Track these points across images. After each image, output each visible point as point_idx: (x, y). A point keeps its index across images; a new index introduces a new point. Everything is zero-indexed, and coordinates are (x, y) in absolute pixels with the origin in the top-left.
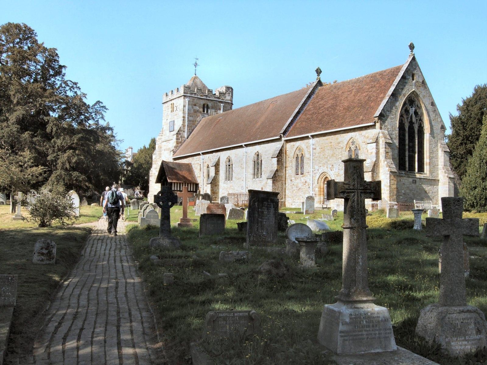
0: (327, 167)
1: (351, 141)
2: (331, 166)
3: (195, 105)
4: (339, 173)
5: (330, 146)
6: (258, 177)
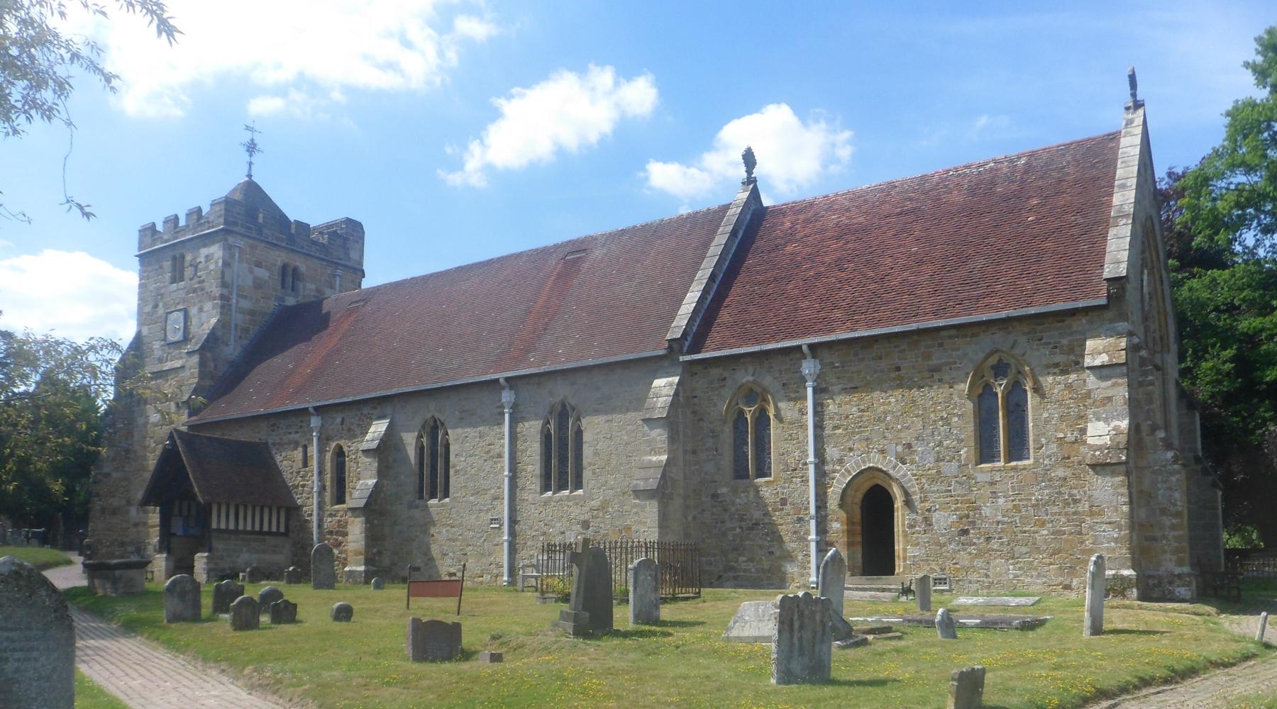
0: (882, 451)
1: (993, 360)
2: (900, 448)
3: (259, 265)
4: (939, 472)
6: (562, 486)
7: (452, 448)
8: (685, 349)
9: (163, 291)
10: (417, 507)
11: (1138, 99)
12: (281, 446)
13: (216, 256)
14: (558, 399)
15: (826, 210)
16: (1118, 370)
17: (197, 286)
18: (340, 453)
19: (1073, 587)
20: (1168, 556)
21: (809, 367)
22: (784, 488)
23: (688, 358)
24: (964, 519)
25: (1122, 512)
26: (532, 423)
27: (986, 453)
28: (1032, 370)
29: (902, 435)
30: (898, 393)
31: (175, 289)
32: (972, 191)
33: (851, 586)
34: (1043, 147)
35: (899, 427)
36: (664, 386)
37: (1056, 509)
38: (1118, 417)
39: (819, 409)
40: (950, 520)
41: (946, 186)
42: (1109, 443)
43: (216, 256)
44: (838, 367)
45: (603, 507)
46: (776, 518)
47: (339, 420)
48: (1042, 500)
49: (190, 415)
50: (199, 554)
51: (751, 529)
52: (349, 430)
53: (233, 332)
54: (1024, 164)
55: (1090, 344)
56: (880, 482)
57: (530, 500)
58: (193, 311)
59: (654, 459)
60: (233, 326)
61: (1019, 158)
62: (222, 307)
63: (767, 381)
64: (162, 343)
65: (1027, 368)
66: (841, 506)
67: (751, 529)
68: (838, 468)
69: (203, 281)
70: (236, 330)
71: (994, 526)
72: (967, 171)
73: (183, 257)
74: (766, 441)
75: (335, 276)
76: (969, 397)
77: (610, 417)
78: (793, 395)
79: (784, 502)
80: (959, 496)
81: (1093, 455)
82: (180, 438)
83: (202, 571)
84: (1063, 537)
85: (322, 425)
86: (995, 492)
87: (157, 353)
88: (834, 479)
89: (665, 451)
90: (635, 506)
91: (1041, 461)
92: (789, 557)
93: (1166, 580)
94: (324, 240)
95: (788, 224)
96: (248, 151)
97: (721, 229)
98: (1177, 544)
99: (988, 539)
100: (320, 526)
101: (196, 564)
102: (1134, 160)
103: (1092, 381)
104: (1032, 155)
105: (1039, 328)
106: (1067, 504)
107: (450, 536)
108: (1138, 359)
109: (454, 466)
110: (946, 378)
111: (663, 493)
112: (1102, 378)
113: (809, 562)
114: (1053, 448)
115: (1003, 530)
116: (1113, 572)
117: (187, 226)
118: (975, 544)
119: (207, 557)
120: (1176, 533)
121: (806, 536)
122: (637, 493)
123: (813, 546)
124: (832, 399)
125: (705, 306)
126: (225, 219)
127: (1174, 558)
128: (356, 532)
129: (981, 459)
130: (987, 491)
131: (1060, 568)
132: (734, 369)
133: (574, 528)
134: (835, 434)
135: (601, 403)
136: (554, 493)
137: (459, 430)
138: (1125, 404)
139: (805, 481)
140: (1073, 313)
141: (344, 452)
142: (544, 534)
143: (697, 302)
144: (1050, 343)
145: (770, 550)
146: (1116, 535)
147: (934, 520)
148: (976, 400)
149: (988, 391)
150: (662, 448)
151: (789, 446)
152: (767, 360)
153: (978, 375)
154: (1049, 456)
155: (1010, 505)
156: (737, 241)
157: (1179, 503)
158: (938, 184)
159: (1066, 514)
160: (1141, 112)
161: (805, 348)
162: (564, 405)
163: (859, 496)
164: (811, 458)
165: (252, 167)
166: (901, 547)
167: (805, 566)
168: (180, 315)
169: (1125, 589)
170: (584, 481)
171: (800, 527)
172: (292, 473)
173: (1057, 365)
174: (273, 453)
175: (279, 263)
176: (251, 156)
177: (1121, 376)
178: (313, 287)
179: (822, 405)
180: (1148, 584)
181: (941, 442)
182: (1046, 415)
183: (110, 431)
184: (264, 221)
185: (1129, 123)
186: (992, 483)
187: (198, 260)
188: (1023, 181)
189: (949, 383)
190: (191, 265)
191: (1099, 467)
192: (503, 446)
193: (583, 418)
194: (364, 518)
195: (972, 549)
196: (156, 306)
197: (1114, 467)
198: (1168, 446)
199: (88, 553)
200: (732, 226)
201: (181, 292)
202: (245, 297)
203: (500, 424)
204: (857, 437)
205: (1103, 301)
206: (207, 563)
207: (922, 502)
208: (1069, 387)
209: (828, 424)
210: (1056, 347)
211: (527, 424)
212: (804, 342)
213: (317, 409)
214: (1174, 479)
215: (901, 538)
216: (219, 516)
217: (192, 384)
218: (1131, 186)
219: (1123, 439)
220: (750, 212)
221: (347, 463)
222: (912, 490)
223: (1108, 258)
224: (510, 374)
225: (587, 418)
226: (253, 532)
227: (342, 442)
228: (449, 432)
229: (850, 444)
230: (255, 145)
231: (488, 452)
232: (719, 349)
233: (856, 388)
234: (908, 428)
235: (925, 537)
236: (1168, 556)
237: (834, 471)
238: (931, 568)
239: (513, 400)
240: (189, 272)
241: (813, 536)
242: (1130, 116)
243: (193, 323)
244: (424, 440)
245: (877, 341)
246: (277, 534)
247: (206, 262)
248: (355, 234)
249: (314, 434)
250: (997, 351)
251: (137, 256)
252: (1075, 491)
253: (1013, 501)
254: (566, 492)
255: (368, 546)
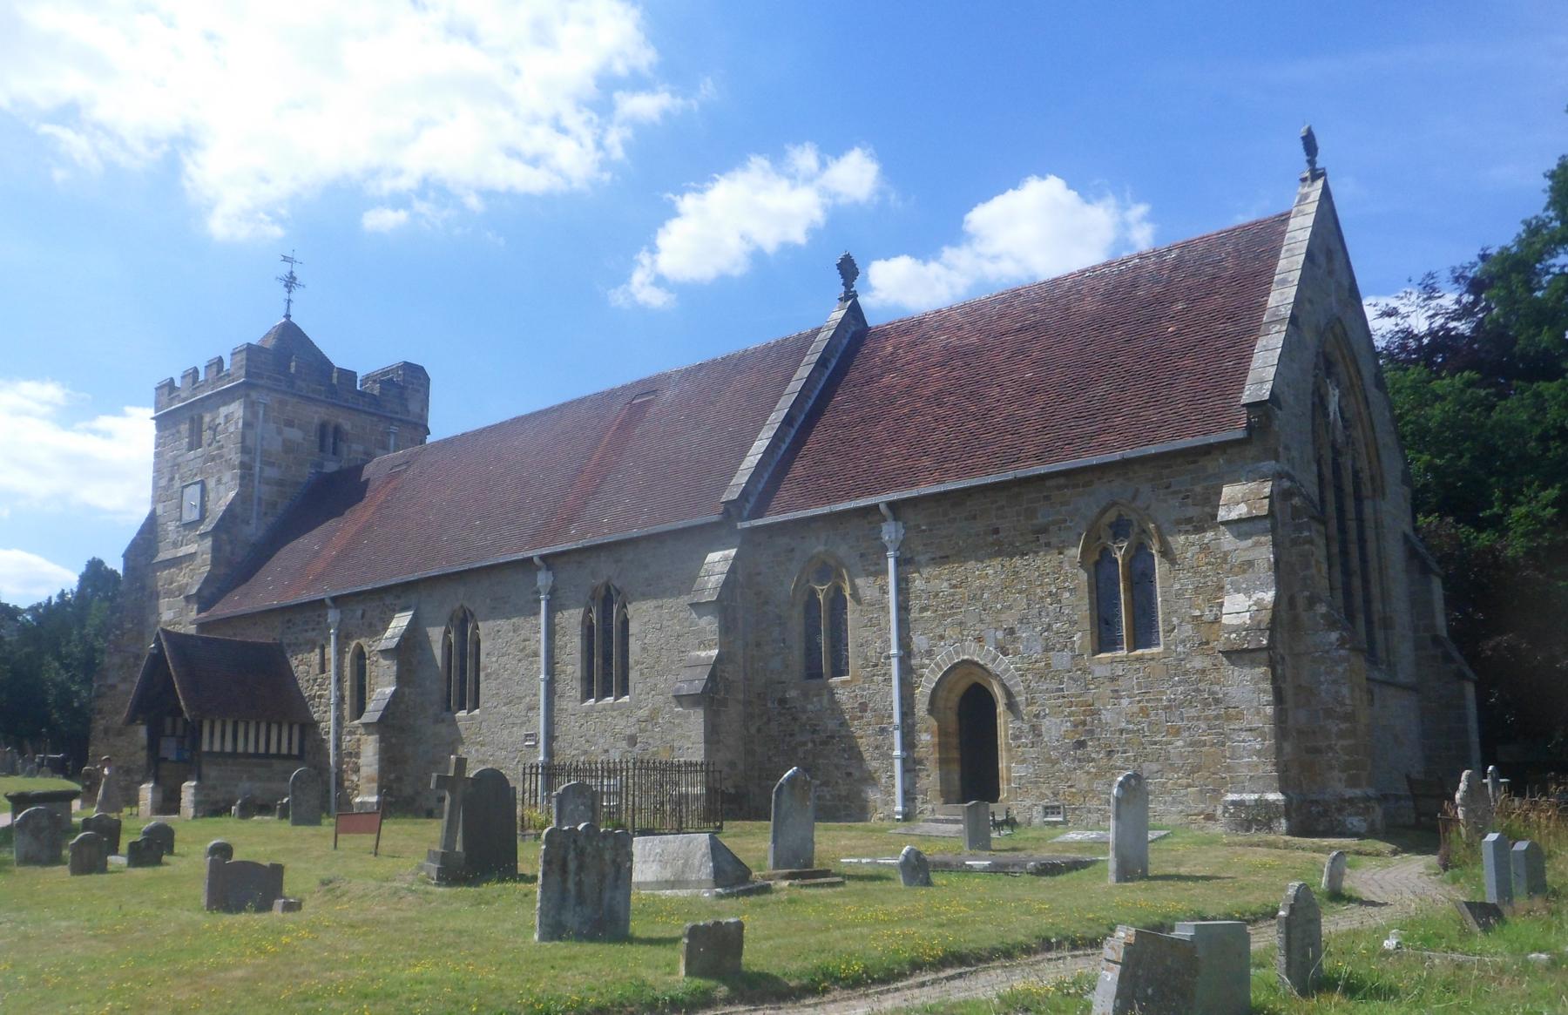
0: (979, 639)
1: (1111, 516)
2: (1000, 635)
3: (290, 423)
4: (1048, 665)
5: (992, 544)
6: (606, 692)
7: (482, 646)
8: (745, 514)
9: (180, 460)
10: (443, 721)
11: (1318, 166)
12: (298, 648)
13: (236, 415)
14: (601, 581)
15: (935, 330)
16: (1261, 525)
17: (216, 452)
18: (360, 656)
19: (1217, 817)
20: (1336, 773)
21: (890, 532)
22: (864, 690)
23: (746, 525)
24: (1080, 727)
25: (1265, 715)
26: (571, 611)
27: (1105, 638)
28: (1158, 528)
29: (1003, 617)
30: (996, 562)
31: (193, 457)
32: (1108, 296)
33: (942, 817)
34: (1201, 235)
35: (999, 606)
36: (718, 560)
37: (1193, 712)
38: (1263, 587)
39: (904, 586)
40: (1063, 729)
41: (1079, 292)
42: (1248, 622)
43: (236, 415)
44: (924, 531)
45: (651, 718)
46: (855, 727)
47: (359, 613)
48: (1175, 699)
49: (199, 612)
50: (186, 784)
51: (824, 743)
52: (370, 625)
53: (255, 507)
54: (1174, 259)
55: (1227, 491)
56: (981, 682)
57: (570, 710)
58: (211, 483)
59: (703, 654)
60: (256, 501)
61: (1170, 250)
62: (242, 477)
63: (842, 550)
64: (178, 523)
65: (1152, 526)
66: (931, 711)
67: (824, 743)
68: (927, 662)
69: (222, 447)
70: (259, 504)
71: (1117, 735)
72: (1106, 270)
73: (201, 418)
74: (844, 627)
75: (389, 434)
76: (1082, 565)
77: (660, 603)
78: (872, 569)
79: (863, 707)
80: (1073, 696)
81: (1228, 638)
82: (166, 640)
83: (188, 804)
84: (1204, 749)
85: (342, 620)
86: (1117, 691)
87: (172, 537)
88: (922, 676)
89: (716, 645)
90: (679, 715)
91: (1173, 647)
92: (870, 779)
93: (1334, 806)
94: (376, 389)
95: (890, 349)
96: (286, 286)
97: (806, 359)
98: (1347, 758)
99: (1110, 753)
100: (338, 747)
101: (183, 795)
102: (1301, 248)
103: (1227, 540)
104: (1185, 246)
105: (1166, 472)
106: (1207, 705)
107: (480, 756)
108: (1289, 510)
109: (486, 668)
110: (1054, 540)
111: (713, 698)
112: (1240, 536)
113: (893, 786)
114: (1188, 629)
115: (1127, 742)
116: (1255, 796)
117: (206, 381)
118: (1093, 760)
119: (195, 786)
120: (1345, 743)
121: (890, 752)
122: (680, 699)
123: (898, 764)
124: (919, 572)
125: (777, 458)
126: (246, 371)
127: (1344, 776)
128: (369, 752)
129: (1100, 645)
130: (1106, 690)
131: (1201, 791)
132: (803, 538)
133: (618, 745)
134: (923, 617)
135: (650, 585)
136: (597, 701)
137: (491, 623)
138: (1270, 569)
139: (888, 680)
140: (1207, 450)
141: (364, 653)
142: (585, 752)
143: (764, 452)
144: (1180, 492)
145: (849, 770)
146: (1258, 747)
147: (1043, 729)
148: (1093, 569)
149: (1106, 555)
150: (713, 640)
151: (867, 634)
152: (841, 524)
153: (1093, 537)
154: (1183, 642)
155: (1136, 708)
156: (827, 373)
157: (1348, 702)
158: (1070, 288)
159: (1207, 718)
160: (1320, 183)
161: (882, 507)
162: (608, 589)
163: (955, 698)
164: (894, 651)
165: (291, 305)
166: (1004, 764)
167: (889, 792)
168: (197, 488)
169: (1270, 820)
170: (631, 684)
171: (883, 739)
172: (308, 681)
173: (1189, 521)
174: (288, 656)
175: (316, 420)
176: (289, 292)
177: (1264, 533)
178: (361, 448)
179: (906, 580)
180: (1311, 812)
181: (1049, 625)
182: (1177, 586)
183: (118, 632)
184: (296, 371)
185: (1304, 197)
186: (1113, 679)
187: (217, 421)
188: (1170, 281)
189: (1058, 548)
190: (210, 428)
191: (1235, 655)
192: (538, 641)
193: (629, 603)
194: (377, 736)
195: (1091, 767)
196: (172, 479)
197: (1253, 655)
198: (1332, 624)
199: (88, 783)
200: (819, 355)
201: (199, 460)
202: (272, 464)
203: (536, 613)
204: (949, 620)
205: (1239, 434)
206: (195, 795)
207: (1028, 705)
208: (1205, 548)
209: (915, 604)
210: (1187, 497)
211: (566, 613)
212: (881, 499)
213: (334, 599)
214: (1340, 669)
215: (1004, 753)
216: (212, 734)
217: (203, 573)
218: (1293, 281)
219: (1266, 616)
220: (848, 336)
221: (367, 667)
222: (1017, 689)
223: (1251, 376)
224: (545, 551)
225: (634, 603)
226: (256, 755)
227: (362, 641)
228: (480, 624)
229: (940, 631)
230: (295, 279)
231: (521, 651)
232: (784, 512)
233: (947, 557)
234: (1010, 607)
235: (1032, 753)
236: (1336, 773)
237: (922, 666)
238: (1041, 793)
239: (550, 584)
240: (207, 435)
241: (897, 752)
242: (1306, 190)
243: (211, 498)
244: (452, 636)
245: (969, 495)
246: (289, 757)
247: (226, 423)
248: (415, 381)
249: (332, 631)
250: (1114, 504)
251: (153, 419)
252: (1217, 688)
253: (1139, 702)
254: (610, 699)
255: (383, 771)
